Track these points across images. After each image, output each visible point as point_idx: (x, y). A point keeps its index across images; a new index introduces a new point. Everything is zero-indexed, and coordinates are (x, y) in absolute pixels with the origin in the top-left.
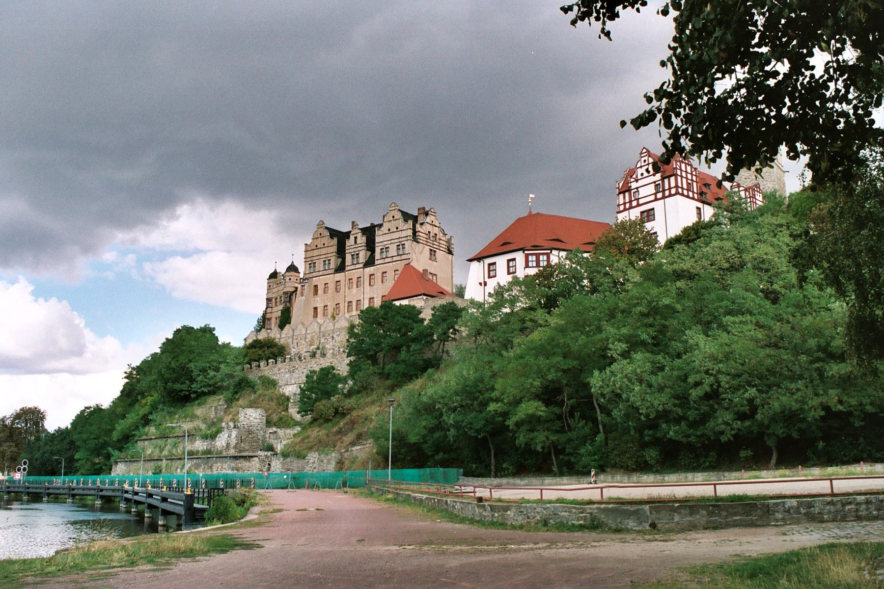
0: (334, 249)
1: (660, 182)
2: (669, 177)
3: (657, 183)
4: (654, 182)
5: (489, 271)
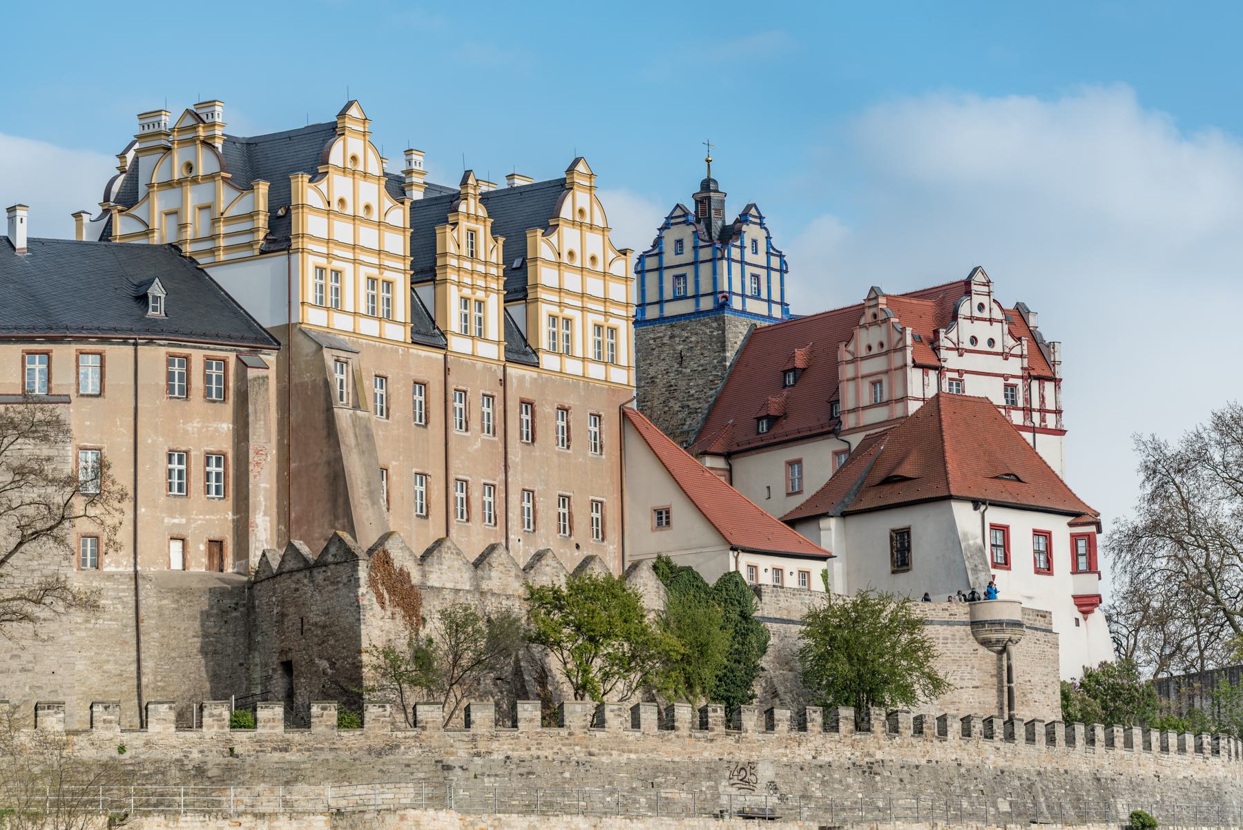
0: (398, 243)
1: (1019, 382)
2: (1041, 379)
3: (1011, 381)
5: (1006, 546)
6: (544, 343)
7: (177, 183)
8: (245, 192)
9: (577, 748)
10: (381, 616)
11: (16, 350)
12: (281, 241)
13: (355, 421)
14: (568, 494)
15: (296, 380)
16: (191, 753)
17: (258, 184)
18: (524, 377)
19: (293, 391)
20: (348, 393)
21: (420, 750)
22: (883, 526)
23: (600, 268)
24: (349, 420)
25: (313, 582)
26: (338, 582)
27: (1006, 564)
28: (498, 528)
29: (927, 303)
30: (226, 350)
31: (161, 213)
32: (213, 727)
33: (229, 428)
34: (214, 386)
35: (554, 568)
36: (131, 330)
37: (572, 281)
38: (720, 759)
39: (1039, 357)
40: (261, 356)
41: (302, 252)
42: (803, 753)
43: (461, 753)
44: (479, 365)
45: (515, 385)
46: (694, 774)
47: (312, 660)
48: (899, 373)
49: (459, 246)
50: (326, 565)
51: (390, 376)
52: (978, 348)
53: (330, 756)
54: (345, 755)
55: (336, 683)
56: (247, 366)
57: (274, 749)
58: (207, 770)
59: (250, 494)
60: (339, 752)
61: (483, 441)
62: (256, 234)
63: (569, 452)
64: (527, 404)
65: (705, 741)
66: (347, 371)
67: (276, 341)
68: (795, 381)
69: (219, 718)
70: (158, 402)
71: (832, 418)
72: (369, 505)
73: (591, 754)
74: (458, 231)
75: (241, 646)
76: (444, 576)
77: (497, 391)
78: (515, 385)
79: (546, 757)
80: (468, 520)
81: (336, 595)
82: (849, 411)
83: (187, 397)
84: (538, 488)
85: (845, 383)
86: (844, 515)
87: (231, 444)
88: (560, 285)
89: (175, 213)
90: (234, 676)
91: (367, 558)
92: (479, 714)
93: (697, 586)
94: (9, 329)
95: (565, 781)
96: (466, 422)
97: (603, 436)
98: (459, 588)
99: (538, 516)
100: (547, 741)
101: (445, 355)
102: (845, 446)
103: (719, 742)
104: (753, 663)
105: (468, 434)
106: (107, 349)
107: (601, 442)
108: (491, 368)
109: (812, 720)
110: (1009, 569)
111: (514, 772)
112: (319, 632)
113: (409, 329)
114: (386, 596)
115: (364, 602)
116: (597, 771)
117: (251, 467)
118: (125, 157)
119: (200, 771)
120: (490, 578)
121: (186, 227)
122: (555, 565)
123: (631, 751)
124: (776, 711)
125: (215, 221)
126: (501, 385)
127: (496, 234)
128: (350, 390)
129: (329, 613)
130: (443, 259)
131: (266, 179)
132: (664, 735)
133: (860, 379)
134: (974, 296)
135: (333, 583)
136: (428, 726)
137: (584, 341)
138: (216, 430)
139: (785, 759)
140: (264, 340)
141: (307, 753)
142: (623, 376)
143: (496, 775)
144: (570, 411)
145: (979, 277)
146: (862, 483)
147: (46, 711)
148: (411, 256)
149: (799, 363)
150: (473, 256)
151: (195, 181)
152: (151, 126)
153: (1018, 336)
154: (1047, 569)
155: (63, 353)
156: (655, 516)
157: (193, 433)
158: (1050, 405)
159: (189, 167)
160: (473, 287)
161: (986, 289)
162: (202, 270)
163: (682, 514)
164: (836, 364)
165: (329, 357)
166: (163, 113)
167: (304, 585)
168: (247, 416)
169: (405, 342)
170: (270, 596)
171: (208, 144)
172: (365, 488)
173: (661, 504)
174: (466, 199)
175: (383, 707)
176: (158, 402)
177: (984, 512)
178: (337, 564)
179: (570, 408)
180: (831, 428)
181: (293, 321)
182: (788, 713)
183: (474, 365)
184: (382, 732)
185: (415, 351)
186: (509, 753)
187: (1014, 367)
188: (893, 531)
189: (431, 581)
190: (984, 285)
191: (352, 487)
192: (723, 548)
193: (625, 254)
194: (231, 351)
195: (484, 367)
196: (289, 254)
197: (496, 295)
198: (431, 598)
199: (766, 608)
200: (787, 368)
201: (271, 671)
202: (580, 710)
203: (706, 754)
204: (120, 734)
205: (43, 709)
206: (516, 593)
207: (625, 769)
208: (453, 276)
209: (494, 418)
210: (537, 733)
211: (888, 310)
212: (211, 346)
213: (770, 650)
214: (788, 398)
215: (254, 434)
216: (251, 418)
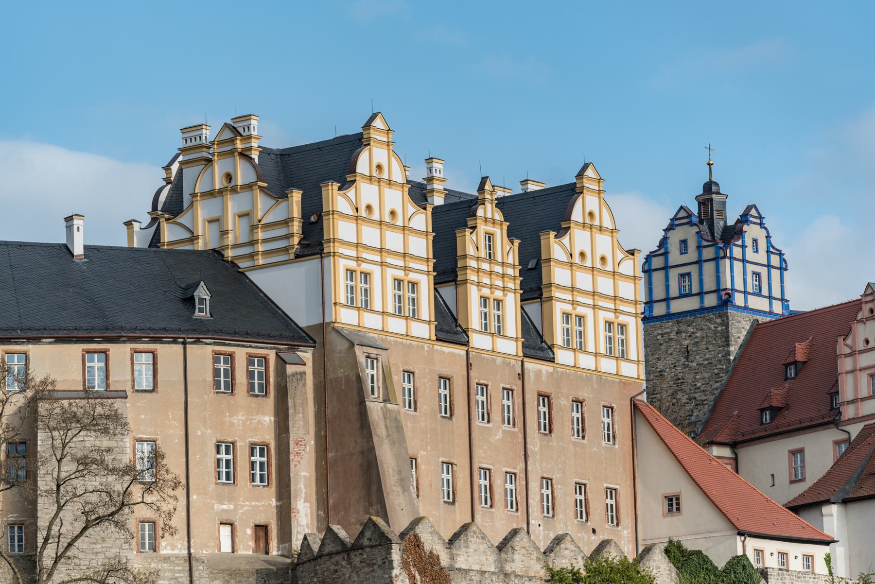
0: (421, 247)
6: (559, 338)
8: (280, 200)
11: (76, 350)
13: (386, 413)
14: (583, 481)
15: (330, 375)
17: (292, 192)
18: (541, 371)
19: (328, 385)
20: (379, 388)
23: (609, 267)
24: (380, 413)
25: (350, 564)
26: (374, 564)
28: (519, 513)
30: (267, 348)
31: (204, 220)
33: (270, 420)
34: (256, 381)
35: (572, 551)
36: (180, 330)
37: (584, 281)
40: (298, 353)
41: (334, 256)
44: (499, 360)
49: (477, 248)
51: (416, 371)
56: (286, 363)
61: (504, 432)
62: (291, 239)
63: (585, 441)
64: (544, 397)
66: (377, 367)
67: (312, 339)
68: (796, 374)
71: (832, 409)
72: (401, 491)
74: (477, 234)
76: (471, 560)
77: (516, 385)
80: (491, 506)
81: (372, 576)
82: (849, 403)
83: (232, 392)
84: (555, 477)
86: (845, 502)
87: (273, 435)
88: (572, 285)
89: (217, 220)
91: (400, 541)
93: (707, 569)
94: (69, 330)
96: (488, 414)
97: (616, 427)
98: (484, 570)
99: (557, 502)
101: (467, 352)
102: (845, 436)
105: (490, 425)
106: (158, 347)
108: (510, 363)
114: (418, 577)
117: (292, 457)
118: (170, 169)
120: (513, 561)
121: (228, 233)
122: (574, 549)
125: (253, 228)
126: (519, 379)
127: (512, 236)
128: (381, 385)
130: (463, 261)
131: (299, 188)
133: (858, 372)
135: (369, 565)
138: (259, 422)
140: (301, 339)
144: (584, 404)
146: (862, 471)
148: (434, 258)
149: (800, 357)
151: (234, 190)
152: (193, 139)
155: (119, 352)
156: (666, 503)
157: (238, 425)
159: (229, 177)
160: (491, 286)
162: (243, 273)
163: (691, 500)
164: (835, 358)
165: (360, 353)
167: (342, 567)
168: (287, 409)
169: (430, 340)
171: (245, 155)
172: (397, 477)
173: (671, 491)
174: (484, 204)
178: (372, 547)
180: (832, 419)
181: (327, 320)
183: (494, 360)
185: (439, 348)
189: (459, 563)
192: (730, 533)
193: (633, 254)
194: (271, 348)
195: (504, 362)
198: (459, 580)
200: (788, 361)
206: (537, 575)
208: (472, 277)
209: (514, 410)
214: (789, 390)
215: (294, 426)
216: (291, 411)
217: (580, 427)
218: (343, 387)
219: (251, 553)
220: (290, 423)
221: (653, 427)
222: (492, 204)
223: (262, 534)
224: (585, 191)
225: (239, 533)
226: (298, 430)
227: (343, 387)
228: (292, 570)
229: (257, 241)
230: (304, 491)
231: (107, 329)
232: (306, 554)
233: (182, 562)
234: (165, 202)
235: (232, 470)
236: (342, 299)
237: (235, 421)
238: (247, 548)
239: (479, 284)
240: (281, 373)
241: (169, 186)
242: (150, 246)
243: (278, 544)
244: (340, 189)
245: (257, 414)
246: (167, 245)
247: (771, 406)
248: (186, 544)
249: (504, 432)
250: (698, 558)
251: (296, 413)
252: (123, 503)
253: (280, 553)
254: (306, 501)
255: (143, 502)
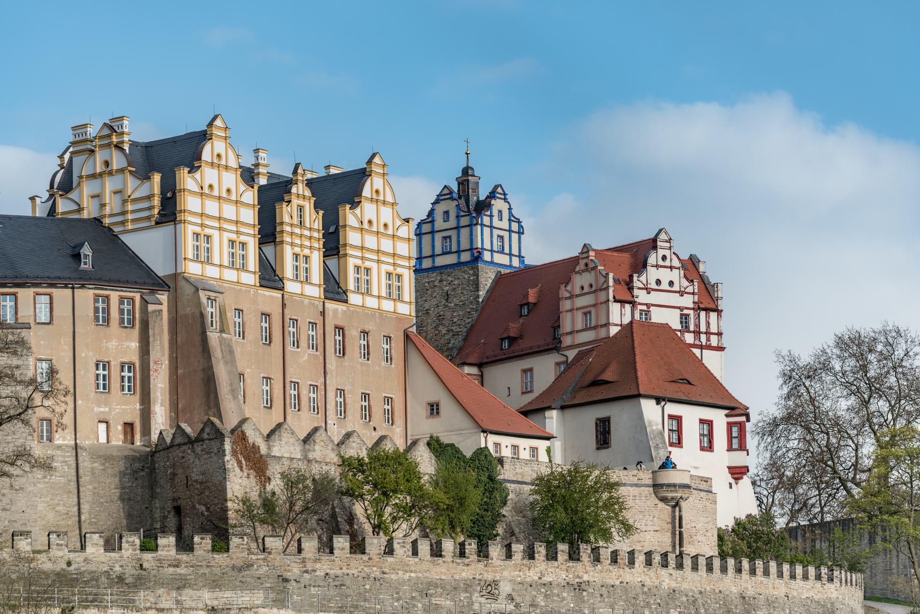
0: (250, 216)
1: (691, 312)
2: (707, 310)
3: (685, 312)
4: (681, 309)
6: (351, 285)
7: (98, 175)
9: (375, 569)
10: (240, 475)
12: (169, 215)
13: (221, 340)
14: (368, 392)
15: (181, 312)
16: (114, 567)
17: (154, 175)
18: (337, 309)
19: (179, 320)
20: (216, 322)
21: (267, 568)
22: (591, 415)
23: (390, 232)
24: (218, 341)
25: (194, 452)
26: (211, 452)
27: (679, 443)
29: (624, 255)
30: (134, 292)
32: (128, 549)
33: (136, 346)
34: (126, 317)
35: (358, 444)
36: (70, 278)
37: (371, 242)
38: (474, 578)
39: (707, 294)
40: (157, 296)
41: (184, 223)
42: (532, 575)
43: (295, 570)
44: (306, 301)
45: (331, 315)
46: (455, 588)
47: (194, 506)
48: (604, 306)
50: (203, 440)
51: (245, 310)
52: (661, 288)
53: (207, 571)
54: (217, 570)
55: (211, 521)
56: (148, 303)
57: (170, 566)
58: (126, 579)
59: (151, 391)
60: (213, 568)
61: (309, 355)
62: (152, 210)
63: (369, 362)
64: (340, 329)
65: (463, 566)
66: (216, 306)
67: (167, 285)
68: (528, 312)
69: (133, 544)
70: (88, 328)
71: (555, 338)
72: (232, 399)
73: (384, 573)
74: (291, 206)
75: (147, 495)
76: (283, 450)
77: (319, 320)
78: (331, 315)
79: (353, 574)
80: (299, 410)
82: (567, 334)
85: (564, 313)
86: (563, 408)
87: (138, 357)
88: (362, 245)
89: (98, 196)
90: (141, 516)
91: (231, 436)
92: (307, 544)
93: (458, 457)
95: (366, 591)
96: (298, 342)
97: (393, 351)
98: (293, 456)
99: (348, 407)
100: (353, 563)
101: (283, 295)
102: (564, 359)
103: (473, 566)
104: (497, 511)
105: (299, 350)
107: (391, 356)
108: (314, 303)
109: (539, 552)
110: (682, 447)
111: (331, 584)
112: (199, 486)
113: (257, 276)
114: (244, 462)
115: (229, 466)
116: (388, 585)
117: (151, 373)
119: (121, 579)
120: (314, 451)
121: (105, 206)
123: (411, 572)
124: (512, 545)
125: (124, 202)
126: (321, 315)
128: (218, 320)
129: (204, 474)
131: (159, 172)
132: (434, 561)
133: (575, 311)
134: (659, 250)
135: (207, 453)
136: (273, 551)
137: (379, 284)
138: (128, 347)
139: (519, 579)
140: (159, 285)
141: (192, 569)
142: (406, 309)
143: (319, 586)
145: (663, 236)
146: (576, 385)
147: (19, 537)
148: (259, 225)
149: (532, 299)
150: (301, 224)
151: (110, 173)
153: (691, 279)
154: (708, 446)
155: (26, 294)
156: (429, 408)
158: (714, 329)
159: (107, 164)
160: (301, 246)
161: (668, 245)
162: (116, 236)
163: (447, 406)
164: (557, 300)
165: (203, 296)
166: (89, 126)
167: (188, 454)
168: (148, 337)
170: (166, 462)
171: (119, 147)
172: (229, 388)
173: (433, 399)
174: (297, 184)
175: (242, 538)
176: (88, 328)
177: (664, 406)
178: (210, 440)
179: (369, 332)
181: (179, 271)
182: (522, 547)
183: (302, 302)
184: (242, 555)
185: (262, 292)
186: (328, 571)
187: (688, 301)
188: (598, 419)
189: (274, 452)
190: (667, 242)
191: (220, 387)
192: (476, 430)
193: (408, 222)
194: (137, 292)
195: (310, 302)
196: (175, 224)
197: (317, 252)
199: (506, 473)
201: (166, 513)
202: (376, 543)
203: (464, 574)
204: (68, 553)
205: (18, 536)
206: (332, 461)
207: (407, 583)
208: (287, 239)
209: (317, 339)
210: (347, 558)
211: (596, 261)
212: (124, 289)
213: (509, 502)
214: (523, 324)
215: (153, 350)
216: (151, 339)
217: (366, 352)
218: (190, 321)
219: (121, 443)
220: (151, 348)
221: (420, 352)
222: (303, 183)
223: (129, 429)
224: (373, 174)
225: (112, 429)
226: (156, 353)
227: (190, 321)
228: (151, 456)
229: (127, 212)
230: (160, 398)
231: (17, 277)
232: (161, 444)
233: (71, 449)
234: (59, 183)
235: (107, 382)
236: (190, 255)
237: (110, 346)
238: (118, 440)
239: (292, 244)
240: (144, 310)
241: (63, 170)
242: (48, 216)
243: (141, 437)
244: (189, 172)
245: (126, 341)
246: (61, 215)
247: (509, 336)
248: (74, 437)
249: (309, 355)
250: (452, 449)
251: (155, 340)
252: (28, 406)
253: (142, 444)
254: (161, 405)
255: (42, 406)
